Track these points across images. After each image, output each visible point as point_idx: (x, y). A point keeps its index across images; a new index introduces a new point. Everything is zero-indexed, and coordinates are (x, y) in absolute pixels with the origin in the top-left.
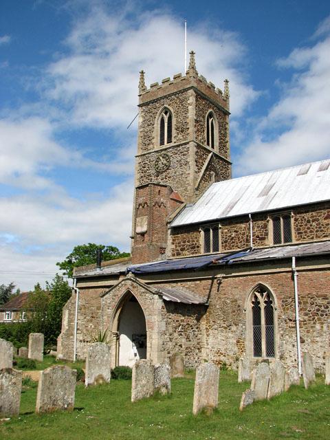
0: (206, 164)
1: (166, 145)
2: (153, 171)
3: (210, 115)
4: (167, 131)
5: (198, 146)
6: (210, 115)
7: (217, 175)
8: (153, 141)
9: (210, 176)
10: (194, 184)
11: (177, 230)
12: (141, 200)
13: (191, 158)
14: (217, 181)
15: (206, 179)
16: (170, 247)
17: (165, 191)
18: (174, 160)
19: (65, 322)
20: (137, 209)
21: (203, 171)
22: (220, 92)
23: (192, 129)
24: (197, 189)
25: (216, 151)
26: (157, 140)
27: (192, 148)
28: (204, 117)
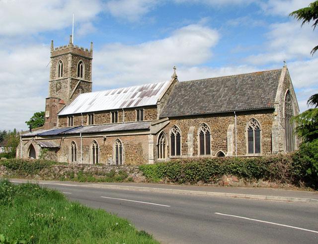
0: (76, 86)
1: (61, 78)
2: (55, 89)
3: (81, 62)
4: (61, 71)
5: (72, 79)
6: (81, 62)
7: (83, 90)
8: (56, 75)
9: (79, 91)
10: (69, 96)
11: (61, 117)
12: (47, 104)
13: (68, 85)
16: (58, 123)
17: (57, 100)
18: (63, 85)
19: (17, 153)
20: (46, 108)
22: (87, 50)
23: (69, 72)
24: (71, 98)
25: (83, 79)
26: (57, 75)
27: (69, 80)
28: (76, 65)
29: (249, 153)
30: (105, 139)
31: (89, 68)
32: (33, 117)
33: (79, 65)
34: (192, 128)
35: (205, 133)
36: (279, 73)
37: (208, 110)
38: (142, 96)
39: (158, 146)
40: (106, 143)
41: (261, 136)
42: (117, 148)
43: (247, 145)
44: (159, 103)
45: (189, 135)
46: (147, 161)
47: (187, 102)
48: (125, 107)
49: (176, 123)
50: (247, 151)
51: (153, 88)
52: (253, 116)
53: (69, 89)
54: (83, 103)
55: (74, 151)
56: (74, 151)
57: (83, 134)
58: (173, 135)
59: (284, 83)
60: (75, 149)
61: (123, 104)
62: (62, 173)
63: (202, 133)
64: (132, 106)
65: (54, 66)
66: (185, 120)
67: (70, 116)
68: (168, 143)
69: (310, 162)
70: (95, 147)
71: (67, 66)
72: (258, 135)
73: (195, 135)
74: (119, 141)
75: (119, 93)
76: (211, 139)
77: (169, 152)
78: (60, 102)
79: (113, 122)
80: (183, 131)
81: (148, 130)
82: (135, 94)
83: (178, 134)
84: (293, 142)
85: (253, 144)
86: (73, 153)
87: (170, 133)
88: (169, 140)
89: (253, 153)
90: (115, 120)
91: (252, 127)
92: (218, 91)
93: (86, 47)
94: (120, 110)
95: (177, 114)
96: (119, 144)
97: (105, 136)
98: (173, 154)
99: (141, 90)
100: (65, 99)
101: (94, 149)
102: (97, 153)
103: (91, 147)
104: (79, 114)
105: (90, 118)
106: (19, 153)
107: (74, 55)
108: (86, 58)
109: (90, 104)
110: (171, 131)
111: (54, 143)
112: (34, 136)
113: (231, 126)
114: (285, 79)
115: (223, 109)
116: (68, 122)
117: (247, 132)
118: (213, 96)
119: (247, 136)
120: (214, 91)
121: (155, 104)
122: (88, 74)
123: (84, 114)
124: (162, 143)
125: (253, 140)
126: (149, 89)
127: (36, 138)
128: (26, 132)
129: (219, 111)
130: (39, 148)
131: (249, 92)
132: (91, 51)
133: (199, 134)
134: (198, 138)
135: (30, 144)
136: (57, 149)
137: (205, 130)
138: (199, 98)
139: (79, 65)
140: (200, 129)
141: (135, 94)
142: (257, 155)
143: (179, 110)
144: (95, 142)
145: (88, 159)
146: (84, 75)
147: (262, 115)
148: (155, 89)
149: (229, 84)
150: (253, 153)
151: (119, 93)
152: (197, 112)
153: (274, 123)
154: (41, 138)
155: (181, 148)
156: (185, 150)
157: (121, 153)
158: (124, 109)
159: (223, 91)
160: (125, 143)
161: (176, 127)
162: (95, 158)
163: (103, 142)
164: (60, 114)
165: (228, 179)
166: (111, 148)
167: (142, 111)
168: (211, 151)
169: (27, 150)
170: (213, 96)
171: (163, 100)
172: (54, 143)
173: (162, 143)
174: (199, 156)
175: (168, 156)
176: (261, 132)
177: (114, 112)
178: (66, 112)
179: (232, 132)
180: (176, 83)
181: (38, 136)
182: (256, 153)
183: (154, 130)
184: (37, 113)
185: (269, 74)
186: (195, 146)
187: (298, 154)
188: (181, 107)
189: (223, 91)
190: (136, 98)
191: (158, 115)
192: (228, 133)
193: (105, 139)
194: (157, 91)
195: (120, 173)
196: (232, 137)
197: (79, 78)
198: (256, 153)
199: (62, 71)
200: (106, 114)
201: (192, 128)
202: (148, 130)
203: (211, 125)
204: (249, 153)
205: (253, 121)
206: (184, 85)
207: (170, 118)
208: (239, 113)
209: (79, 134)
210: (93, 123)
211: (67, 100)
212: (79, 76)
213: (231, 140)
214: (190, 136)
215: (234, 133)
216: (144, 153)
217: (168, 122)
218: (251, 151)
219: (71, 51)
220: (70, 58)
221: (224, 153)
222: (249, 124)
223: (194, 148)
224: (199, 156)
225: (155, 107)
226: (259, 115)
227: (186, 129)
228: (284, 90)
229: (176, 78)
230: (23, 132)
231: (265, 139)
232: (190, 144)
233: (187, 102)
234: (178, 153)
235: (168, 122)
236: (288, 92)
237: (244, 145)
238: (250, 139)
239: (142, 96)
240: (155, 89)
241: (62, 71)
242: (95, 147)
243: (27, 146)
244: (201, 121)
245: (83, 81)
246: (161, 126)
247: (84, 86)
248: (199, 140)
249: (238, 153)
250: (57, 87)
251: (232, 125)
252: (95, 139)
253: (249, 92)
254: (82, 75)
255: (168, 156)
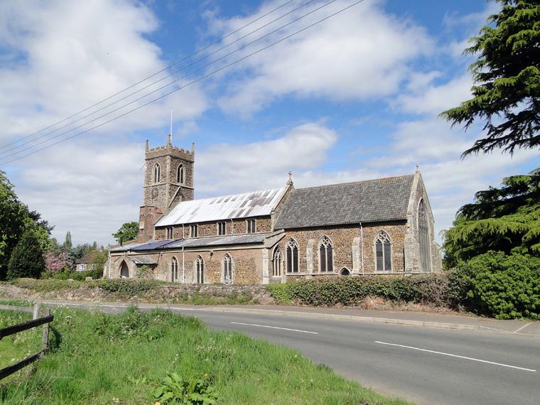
1: (157, 183)
3: (181, 166)
4: (158, 174)
6: (181, 166)
7: (183, 197)
9: (178, 199)
11: (158, 228)
12: (142, 213)
13: (167, 192)
14: (183, 200)
15: (175, 201)
16: (154, 235)
17: (153, 209)
18: (160, 191)
19: (105, 272)
20: (140, 217)
21: (173, 197)
22: (188, 152)
25: (184, 185)
27: (168, 186)
29: (378, 270)
30: (212, 254)
31: (190, 171)
32: (122, 229)
33: (179, 169)
34: (311, 241)
35: (326, 247)
36: (411, 179)
37: (330, 220)
38: (253, 205)
39: (273, 261)
40: (213, 259)
41: (392, 251)
42: (226, 264)
43: (375, 261)
44: (273, 213)
45: (308, 249)
46: (261, 279)
47: (304, 211)
48: (234, 217)
49: (292, 235)
50: (376, 268)
51: (266, 195)
52: (381, 228)
53: (167, 196)
54: (183, 213)
55: (175, 268)
56: (175, 268)
57: (185, 248)
58: (289, 249)
59: (417, 190)
60: (176, 266)
61: (231, 214)
62: (173, 294)
63: (323, 248)
64: (242, 216)
65: (149, 170)
66: (303, 232)
67: (169, 227)
68: (284, 258)
69: (471, 283)
70: (200, 263)
71: (166, 170)
72: (388, 250)
73: (315, 249)
74: (228, 256)
75: (226, 201)
76: (334, 254)
77: (284, 269)
78: (158, 211)
79: (220, 234)
80: (301, 245)
81: (262, 243)
82: (245, 202)
83: (296, 248)
84: (429, 257)
85: (382, 261)
86: (173, 270)
87: (286, 247)
88: (284, 255)
89: (382, 270)
90: (222, 232)
91: (381, 240)
92: (340, 199)
93: (187, 148)
94: (228, 221)
95: (295, 225)
96: (228, 260)
97: (212, 250)
98: (290, 270)
99: (252, 198)
100: (163, 208)
101: (198, 265)
102: (202, 270)
103: (196, 263)
104: (180, 225)
105: (193, 229)
106: (108, 271)
107: (173, 158)
108: (187, 161)
109: (193, 213)
110: (287, 244)
111: (151, 259)
112: (126, 251)
113: (357, 240)
114: (418, 185)
115: (347, 220)
116: (166, 234)
117: (375, 246)
118: (335, 205)
119: (375, 251)
120: (336, 200)
121: (268, 213)
122: (189, 179)
123: (186, 225)
124: (278, 258)
125: (382, 256)
126: (261, 197)
127: (129, 253)
128: (116, 246)
129: (342, 222)
130: (133, 265)
131: (377, 201)
132: (193, 153)
133: (319, 248)
134: (319, 252)
135: (121, 260)
136: (154, 266)
137: (326, 243)
138: (318, 207)
139: (179, 169)
140: (321, 242)
141: (245, 202)
142: (387, 272)
143: (296, 221)
144: (200, 258)
145: (191, 277)
146: (184, 180)
147: (393, 226)
148: (267, 197)
149: (352, 191)
150: (382, 270)
151: (226, 201)
152: (317, 224)
153: (407, 237)
154: (134, 253)
155: (299, 264)
156: (304, 267)
157: (230, 270)
158: (233, 219)
159: (346, 199)
160: (235, 258)
161: (292, 240)
162: (201, 277)
163: (209, 257)
164: (158, 225)
165: (372, 301)
166: (219, 264)
167: (254, 221)
168: (334, 267)
169: (117, 267)
170: (335, 205)
171: (277, 210)
172: (151, 259)
173: (278, 258)
174: (319, 273)
175: (284, 273)
176: (392, 246)
177: (222, 222)
178: (164, 222)
179: (357, 246)
180: (291, 191)
181: (131, 250)
182: (386, 270)
183: (268, 243)
184: (126, 224)
185: (399, 180)
186: (315, 262)
187: (455, 274)
188: (298, 218)
189: (346, 199)
190: (247, 208)
191: (272, 226)
192: (353, 247)
193: (212, 254)
194: (271, 199)
195: (244, 293)
196: (358, 251)
197: (178, 184)
198: (386, 270)
199: (159, 175)
200: (212, 225)
201: (311, 241)
202: (262, 243)
203: (333, 237)
204: (378, 270)
205: (383, 234)
206: (300, 193)
207: (286, 230)
208: (365, 225)
209: (180, 248)
210: (196, 236)
211: (166, 209)
212: (178, 181)
213: (356, 255)
214: (309, 250)
215: (361, 247)
216: (257, 270)
217: (284, 234)
218: (380, 267)
219: (170, 153)
220: (169, 161)
221: (349, 270)
222: (377, 237)
223: (314, 264)
224: (319, 272)
225: (268, 217)
226: (389, 227)
227: (304, 243)
228: (417, 199)
229: (291, 184)
230: (112, 247)
231: (396, 254)
232: (309, 259)
233: (304, 211)
234: (296, 270)
235: (284, 234)
236: (422, 201)
237: (371, 260)
238: (379, 254)
239: (253, 205)
240: (267, 197)
241: (159, 175)
242: (200, 263)
243: (118, 263)
244: (322, 233)
245: (183, 187)
246: (276, 239)
247: (184, 193)
248: (319, 255)
249: (366, 270)
250: (153, 194)
251: (357, 238)
252: (200, 254)
253: (377, 201)
254: (182, 180)
255: (284, 273)
